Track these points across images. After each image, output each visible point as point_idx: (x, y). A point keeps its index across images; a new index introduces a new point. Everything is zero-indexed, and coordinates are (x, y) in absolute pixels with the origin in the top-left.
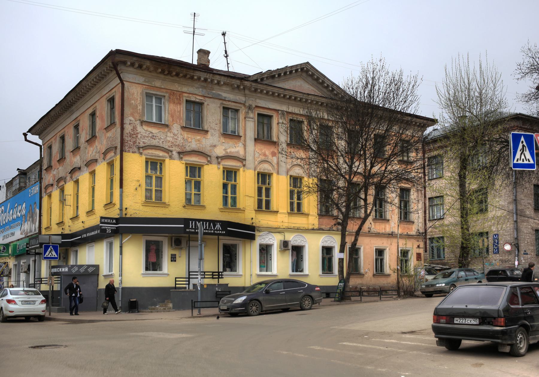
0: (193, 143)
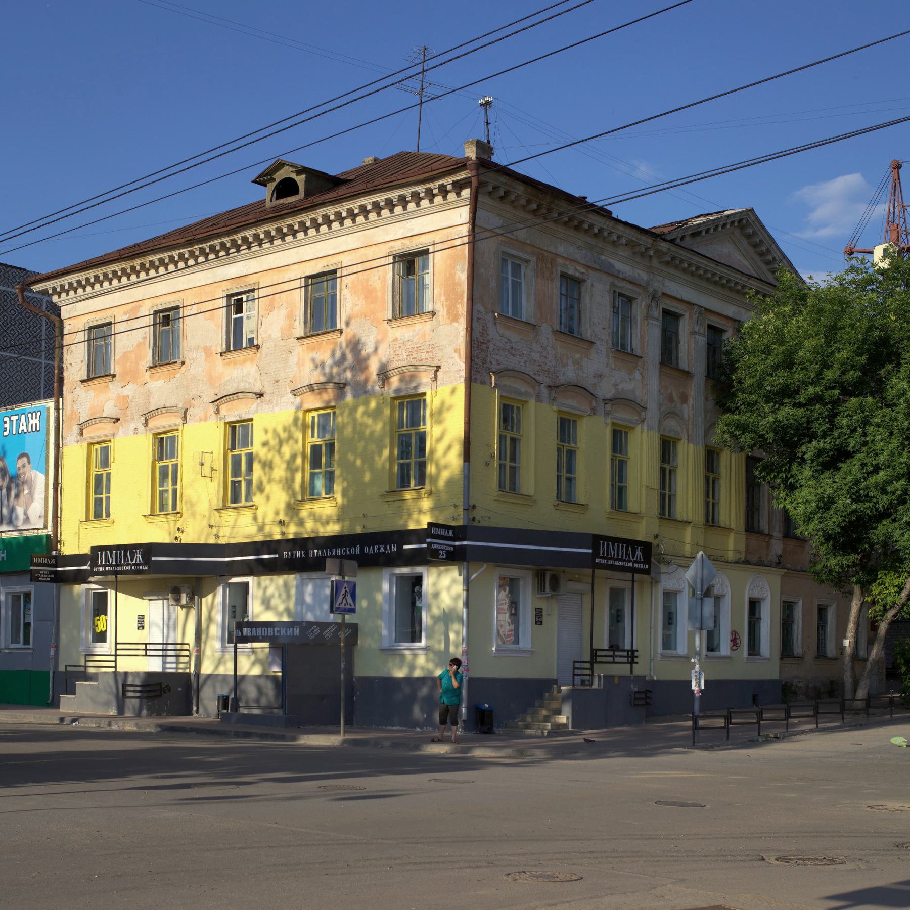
0: (569, 367)
